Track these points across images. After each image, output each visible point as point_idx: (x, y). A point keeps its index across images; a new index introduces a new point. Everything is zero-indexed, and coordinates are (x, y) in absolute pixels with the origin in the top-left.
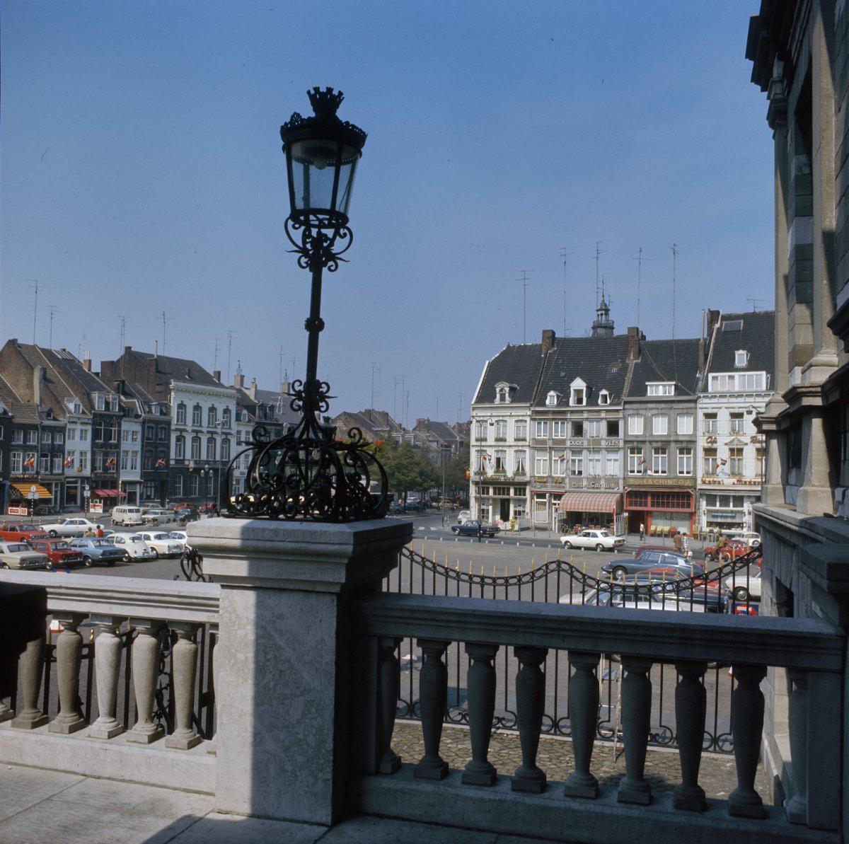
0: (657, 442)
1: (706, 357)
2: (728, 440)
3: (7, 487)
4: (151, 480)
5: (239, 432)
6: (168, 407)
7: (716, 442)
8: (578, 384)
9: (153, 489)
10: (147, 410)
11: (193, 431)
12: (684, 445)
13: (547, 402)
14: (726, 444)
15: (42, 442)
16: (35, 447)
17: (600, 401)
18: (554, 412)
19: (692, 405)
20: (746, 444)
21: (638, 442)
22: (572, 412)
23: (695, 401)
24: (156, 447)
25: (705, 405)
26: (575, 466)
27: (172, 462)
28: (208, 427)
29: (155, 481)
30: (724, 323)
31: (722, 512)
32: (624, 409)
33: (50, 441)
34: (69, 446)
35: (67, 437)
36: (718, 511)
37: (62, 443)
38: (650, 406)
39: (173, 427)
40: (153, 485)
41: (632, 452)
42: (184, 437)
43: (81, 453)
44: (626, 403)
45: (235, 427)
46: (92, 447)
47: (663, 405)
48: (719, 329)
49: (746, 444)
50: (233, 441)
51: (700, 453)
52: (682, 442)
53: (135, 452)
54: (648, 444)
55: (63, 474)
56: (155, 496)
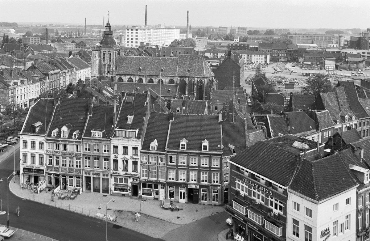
0: (95, 156)
1: (117, 116)
2: (123, 156)
7: (117, 157)
8: (64, 129)
12: (106, 158)
13: (52, 135)
14: (122, 159)
17: (73, 137)
18: (54, 140)
19: (109, 142)
20: (129, 159)
21: (88, 155)
22: (62, 141)
23: (110, 141)
25: (114, 142)
26: (63, 162)
30: (127, 97)
31: (120, 184)
32: (83, 141)
36: (118, 184)
38: (92, 141)
41: (86, 158)
44: (83, 139)
47: (98, 141)
48: (124, 100)
49: (129, 159)
51: (112, 162)
52: (105, 156)
54: (92, 157)
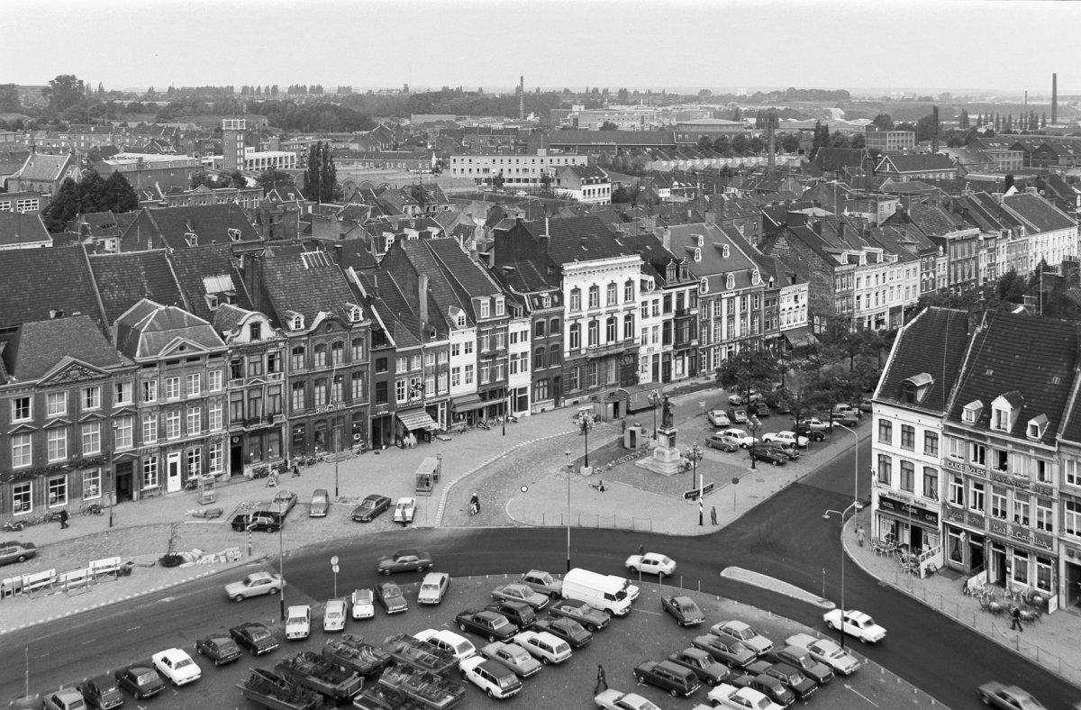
3: (393, 419)
4: (543, 380)
5: (644, 303)
6: (561, 295)
9: (546, 389)
10: (537, 303)
11: (589, 315)
15: (427, 365)
16: (419, 371)
24: (548, 343)
27: (567, 355)
28: (608, 306)
29: (547, 379)
33: (434, 364)
34: (452, 366)
35: (451, 354)
37: (446, 361)
39: (566, 317)
40: (546, 383)
42: (580, 324)
43: (467, 367)
45: (639, 298)
46: (478, 359)
50: (637, 314)
53: (524, 354)
55: (448, 394)
56: (548, 395)
